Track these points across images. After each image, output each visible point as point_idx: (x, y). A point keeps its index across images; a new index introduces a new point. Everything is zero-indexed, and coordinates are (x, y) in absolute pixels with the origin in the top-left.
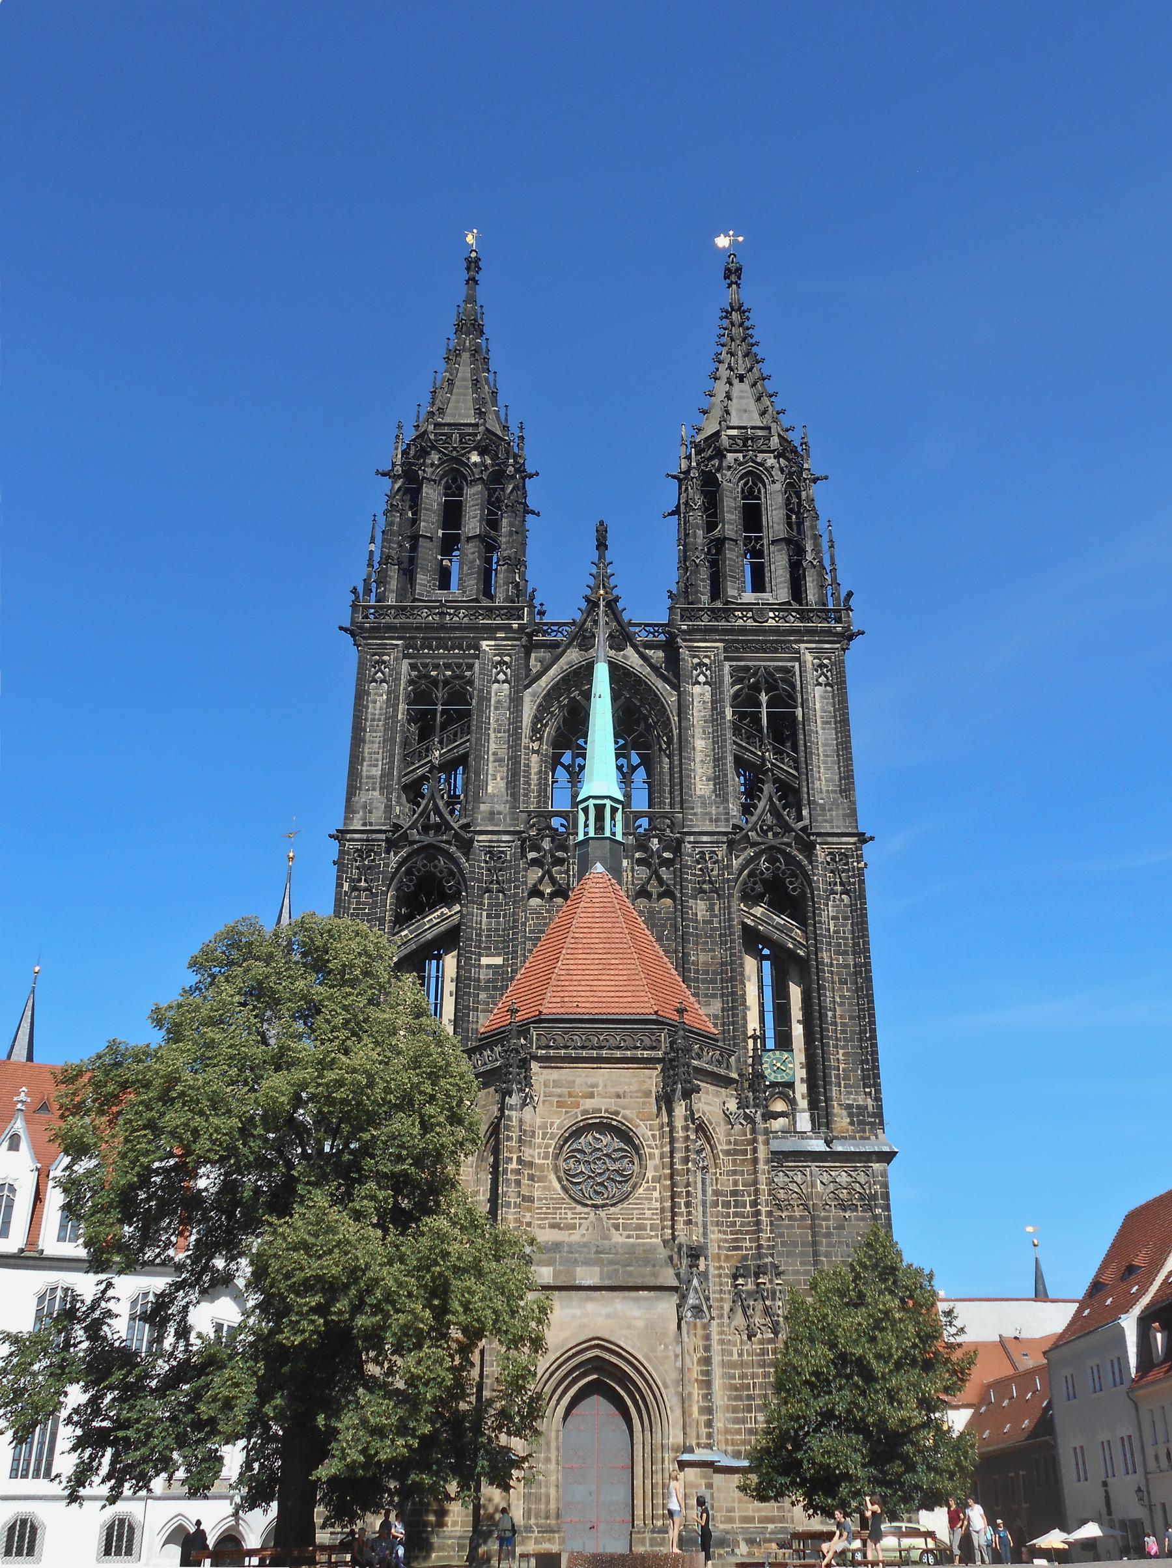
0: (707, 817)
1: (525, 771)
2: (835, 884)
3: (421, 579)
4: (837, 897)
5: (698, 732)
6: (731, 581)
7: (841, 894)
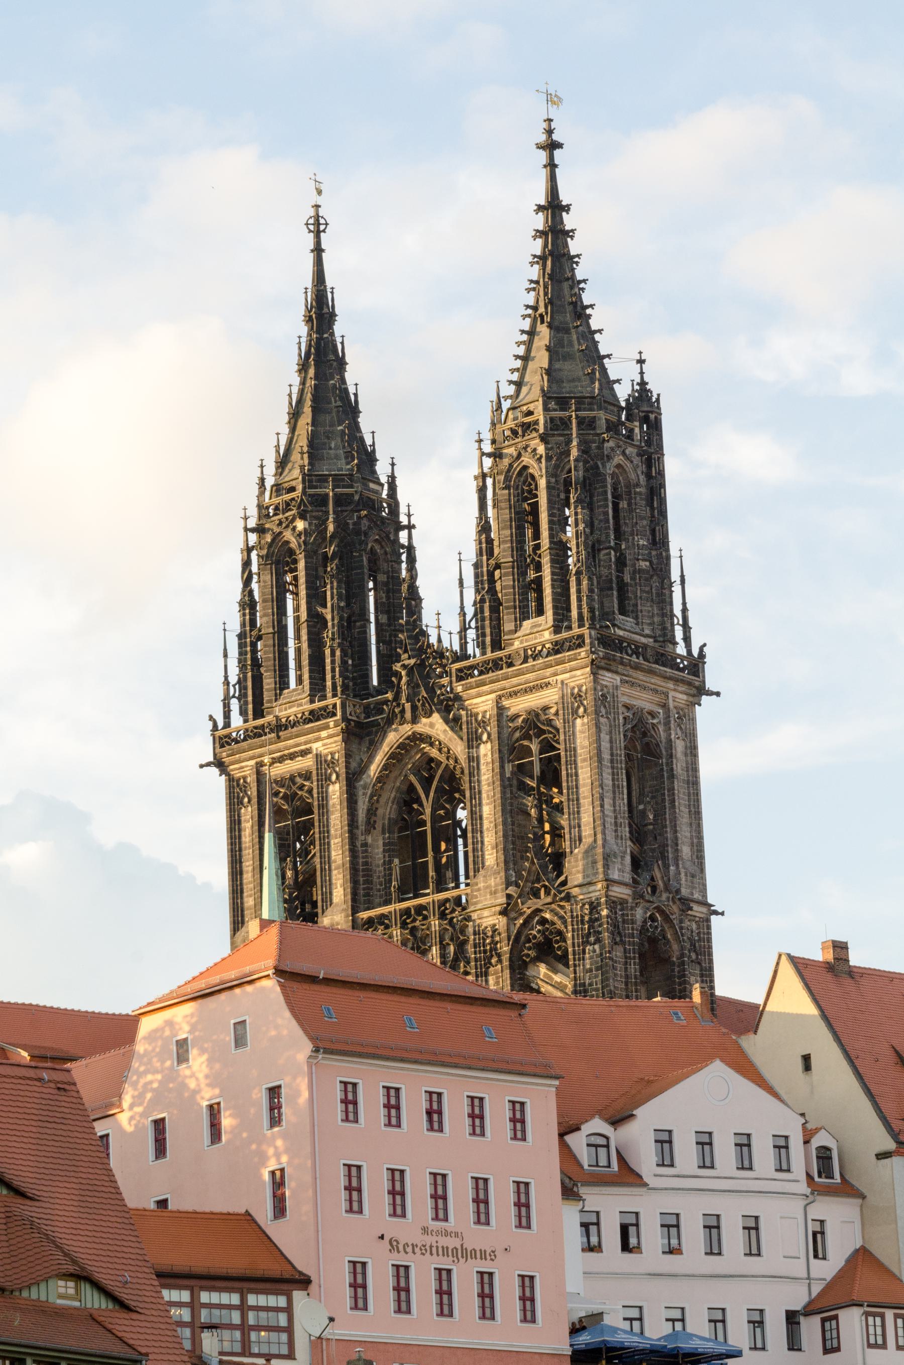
0: (488, 890)
1: (363, 870)
2: (589, 934)
3: (268, 684)
4: (591, 948)
5: (484, 795)
6: (508, 614)
7: (594, 944)
